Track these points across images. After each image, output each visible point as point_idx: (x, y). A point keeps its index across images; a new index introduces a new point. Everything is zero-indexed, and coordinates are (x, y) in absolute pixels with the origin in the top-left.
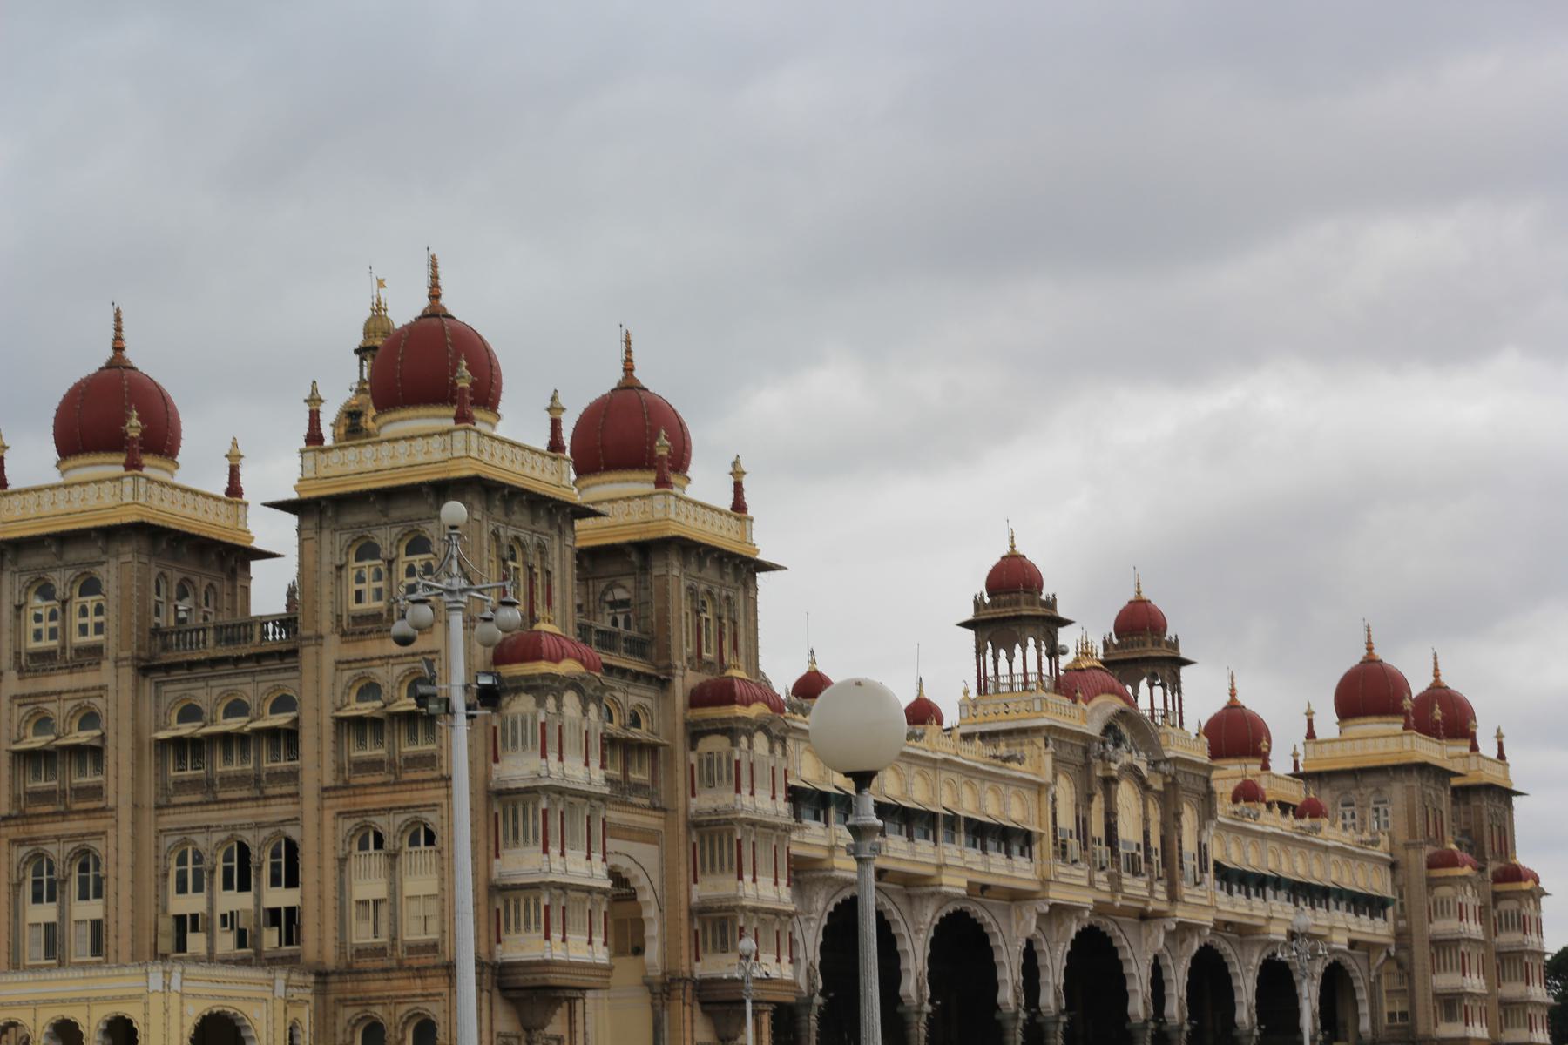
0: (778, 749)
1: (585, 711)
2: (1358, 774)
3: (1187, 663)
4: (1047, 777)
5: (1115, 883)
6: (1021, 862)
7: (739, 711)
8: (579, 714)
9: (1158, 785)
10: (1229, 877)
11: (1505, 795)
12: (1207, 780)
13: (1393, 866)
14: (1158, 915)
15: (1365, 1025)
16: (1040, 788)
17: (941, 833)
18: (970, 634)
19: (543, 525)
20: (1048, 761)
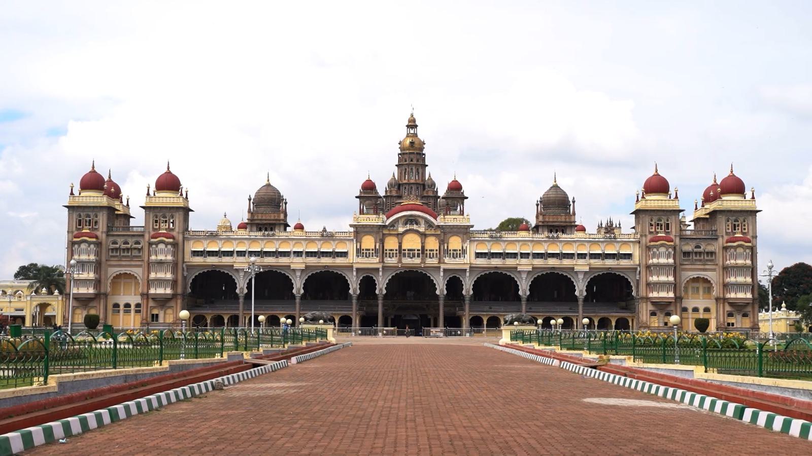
1: (89, 246)
3: (467, 198)
5: (400, 261)
9: (439, 232)
15: (634, 293)
16: (353, 240)
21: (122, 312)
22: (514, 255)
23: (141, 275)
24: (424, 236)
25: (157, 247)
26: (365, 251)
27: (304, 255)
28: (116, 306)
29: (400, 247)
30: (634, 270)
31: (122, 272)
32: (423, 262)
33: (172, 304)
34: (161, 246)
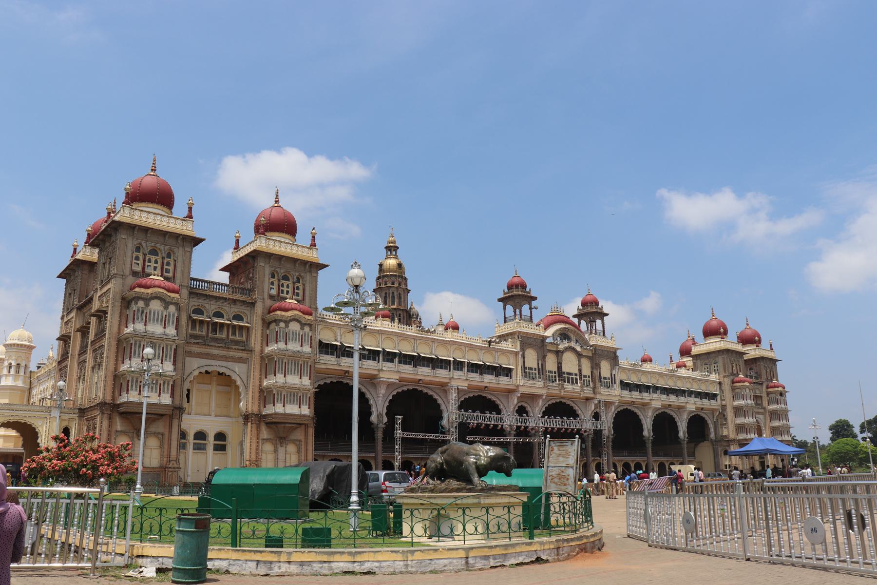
0: (307, 329)
1: (166, 308)
2: (708, 354)
3: (607, 315)
4: (518, 349)
6: (505, 378)
7: (278, 313)
8: (162, 308)
9: (590, 355)
10: (625, 385)
11: (774, 361)
12: (615, 353)
13: (720, 383)
14: (592, 398)
15: (712, 435)
16: (516, 353)
17: (452, 367)
18: (502, 304)
19: (172, 241)
20: (519, 343)
21: (190, 447)
22: (647, 388)
23: (244, 378)
24: (579, 355)
25: (287, 326)
26: (527, 371)
27: (465, 369)
28: (183, 435)
29: (560, 368)
30: (713, 411)
31: (210, 369)
32: (582, 390)
33: (299, 435)
34: (294, 327)
